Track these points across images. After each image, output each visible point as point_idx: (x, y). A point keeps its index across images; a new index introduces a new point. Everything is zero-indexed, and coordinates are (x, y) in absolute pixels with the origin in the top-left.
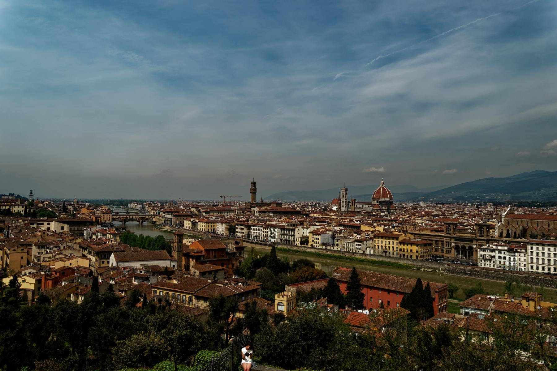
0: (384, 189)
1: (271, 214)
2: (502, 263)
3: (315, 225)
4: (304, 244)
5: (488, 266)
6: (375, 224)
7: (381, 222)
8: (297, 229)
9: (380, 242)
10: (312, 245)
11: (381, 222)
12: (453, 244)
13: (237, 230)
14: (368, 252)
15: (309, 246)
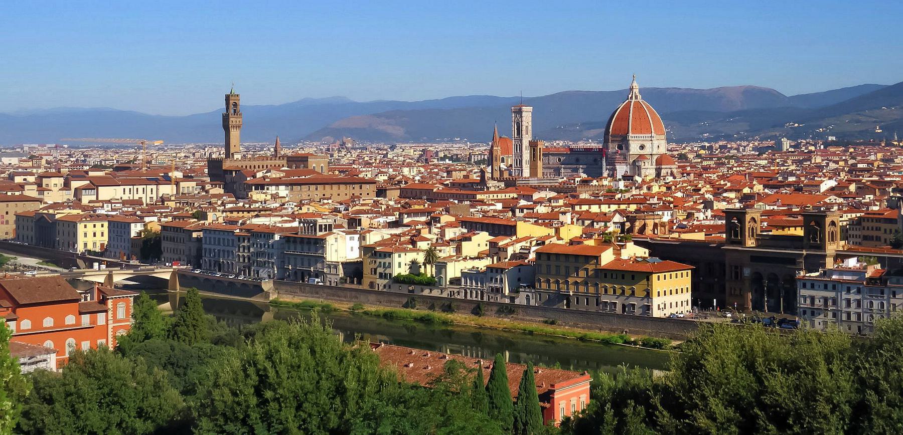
0: (638, 106)
1: (283, 191)
2: (853, 318)
3: (396, 224)
4: (352, 282)
5: (819, 327)
6: (562, 218)
7: (595, 209)
8: (330, 240)
9: (553, 271)
10: (372, 284)
11: (595, 209)
12: (747, 272)
13: (165, 245)
14: (521, 300)
15: (365, 286)
